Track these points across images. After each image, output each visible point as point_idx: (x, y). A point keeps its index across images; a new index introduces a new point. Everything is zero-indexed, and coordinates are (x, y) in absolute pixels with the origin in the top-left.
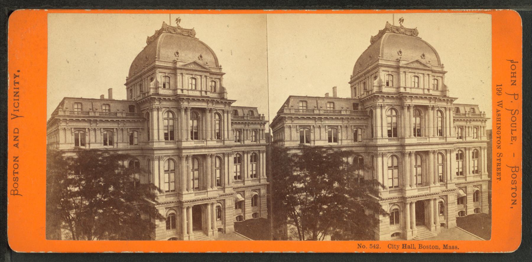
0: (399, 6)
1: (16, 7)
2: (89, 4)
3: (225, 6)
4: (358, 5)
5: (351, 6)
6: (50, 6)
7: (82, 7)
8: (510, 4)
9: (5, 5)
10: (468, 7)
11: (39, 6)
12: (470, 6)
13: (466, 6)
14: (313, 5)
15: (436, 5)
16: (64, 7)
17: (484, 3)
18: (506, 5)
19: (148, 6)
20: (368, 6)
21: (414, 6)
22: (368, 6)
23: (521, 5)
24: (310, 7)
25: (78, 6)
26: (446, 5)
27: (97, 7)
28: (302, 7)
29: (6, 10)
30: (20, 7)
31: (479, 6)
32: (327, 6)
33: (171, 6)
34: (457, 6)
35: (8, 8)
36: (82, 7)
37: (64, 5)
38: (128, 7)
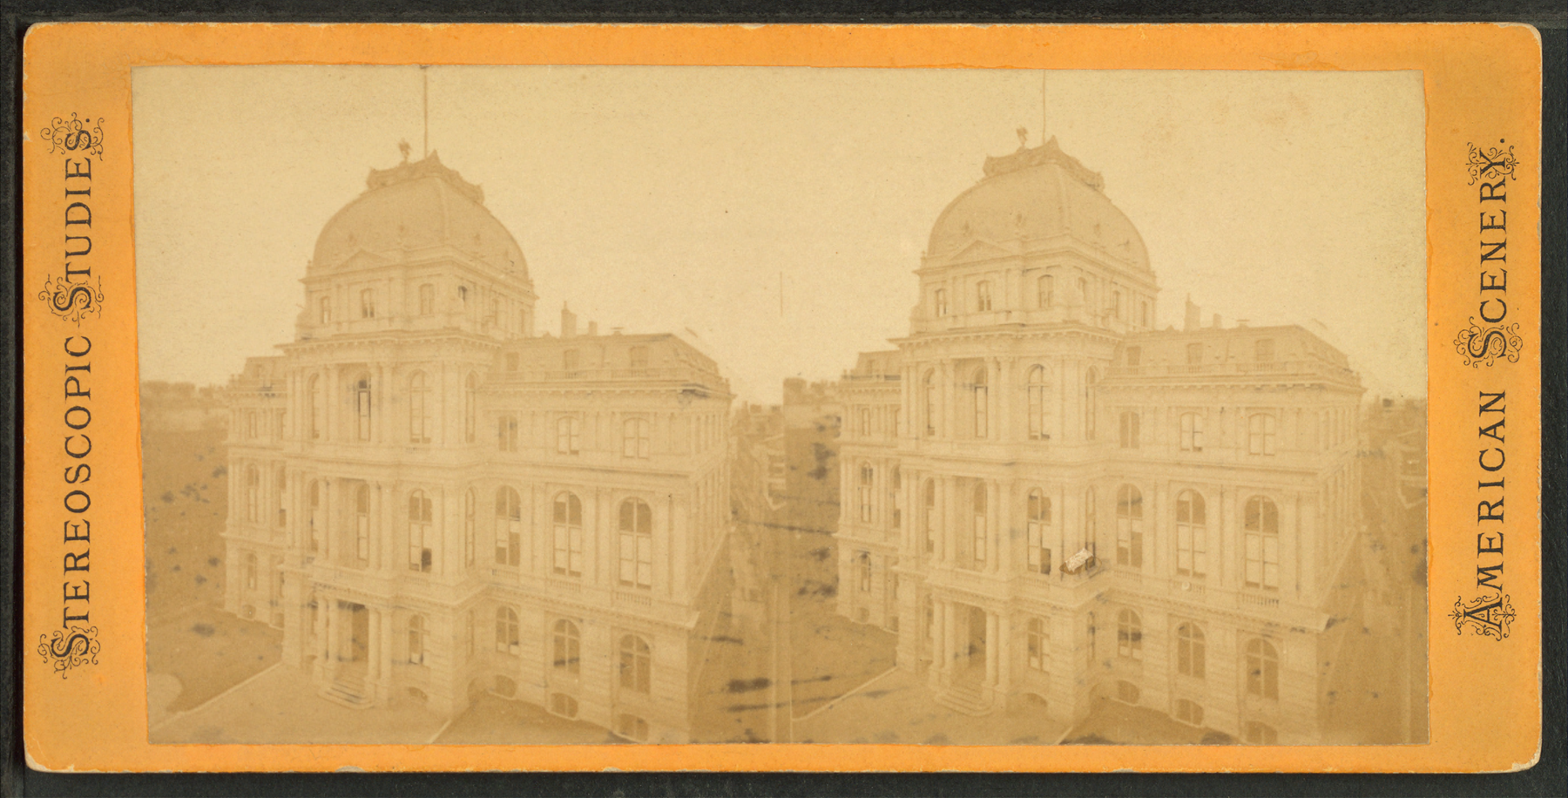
0: (1170, 14)
1: (42, 13)
2: (257, 5)
3: (655, 13)
4: (1050, 9)
5: (1028, 13)
6: (141, 10)
7: (235, 14)
8: (1498, 7)
9: (9, 7)
10: (1373, 16)
11: (109, 11)
12: (1379, 15)
13: (1367, 13)
14: (917, 9)
15: (1278, 11)
16: (183, 14)
17: (1420, 6)
18: (1484, 12)
19: (430, 10)
20: (1077, 13)
21: (1215, 15)
22: (1077, 13)
23: (1528, 12)
24: (904, 15)
25: (223, 11)
26: (1310, 11)
27: (279, 13)
28: (885, 15)
29: (12, 23)
30: (54, 14)
31: (1406, 13)
32: (958, 14)
33: (497, 11)
34: (1340, 15)
35: (16, 17)
36: (235, 14)
37: (180, 9)
38: (371, 14)
